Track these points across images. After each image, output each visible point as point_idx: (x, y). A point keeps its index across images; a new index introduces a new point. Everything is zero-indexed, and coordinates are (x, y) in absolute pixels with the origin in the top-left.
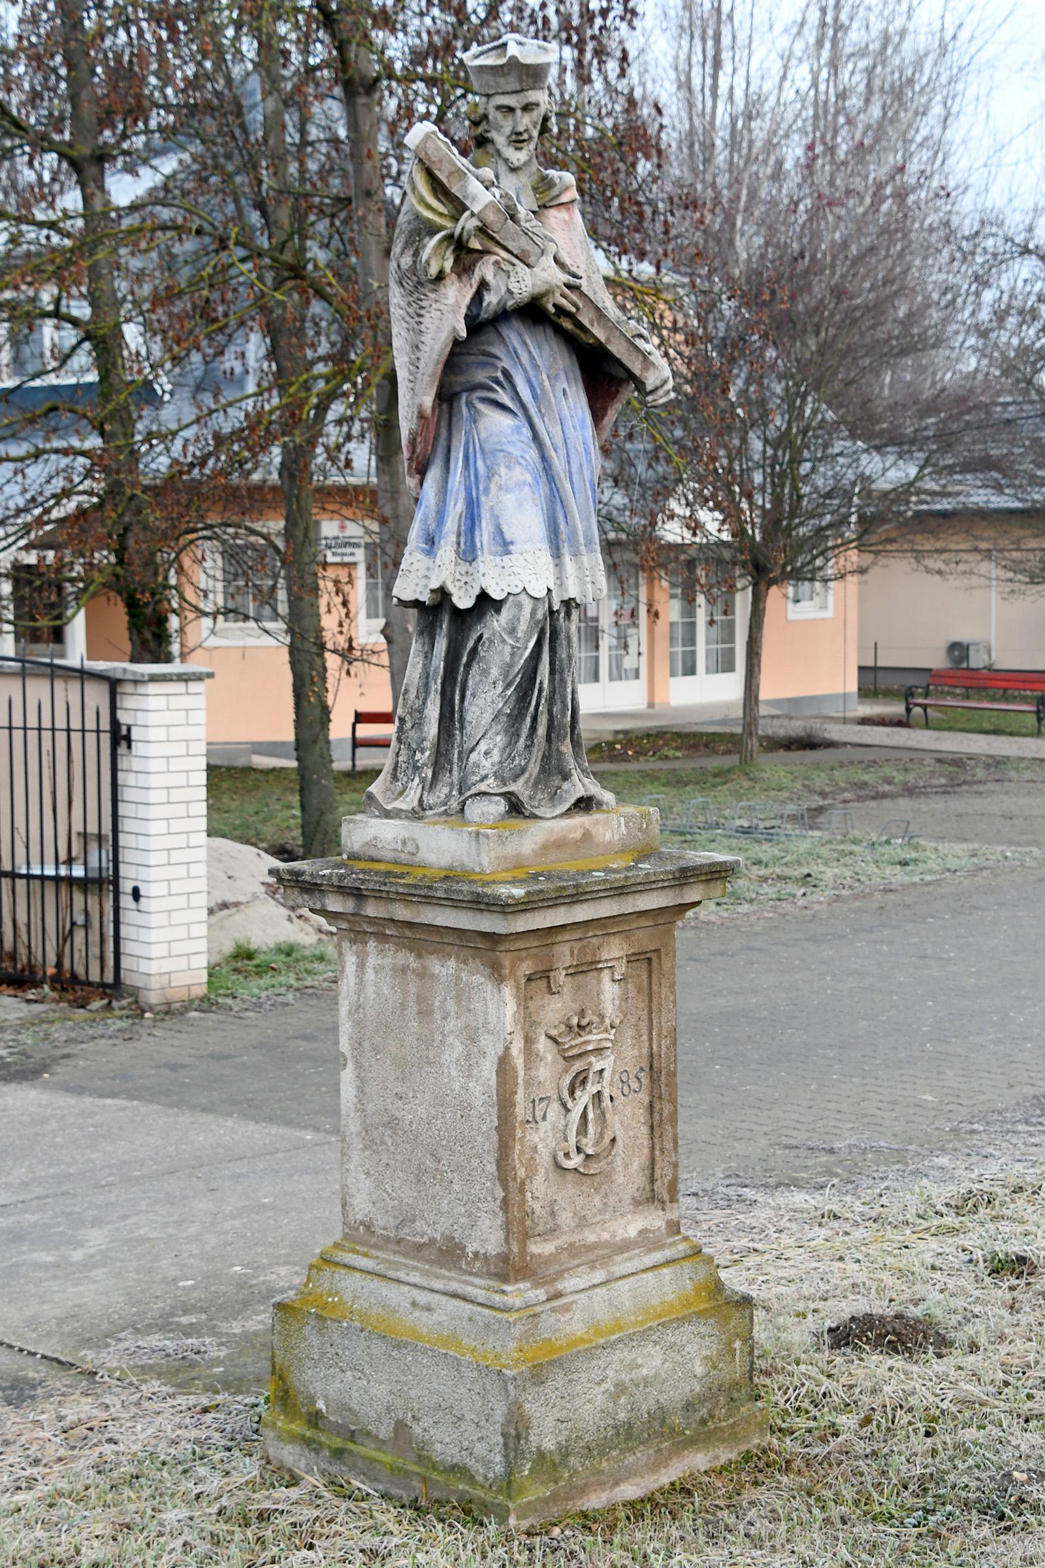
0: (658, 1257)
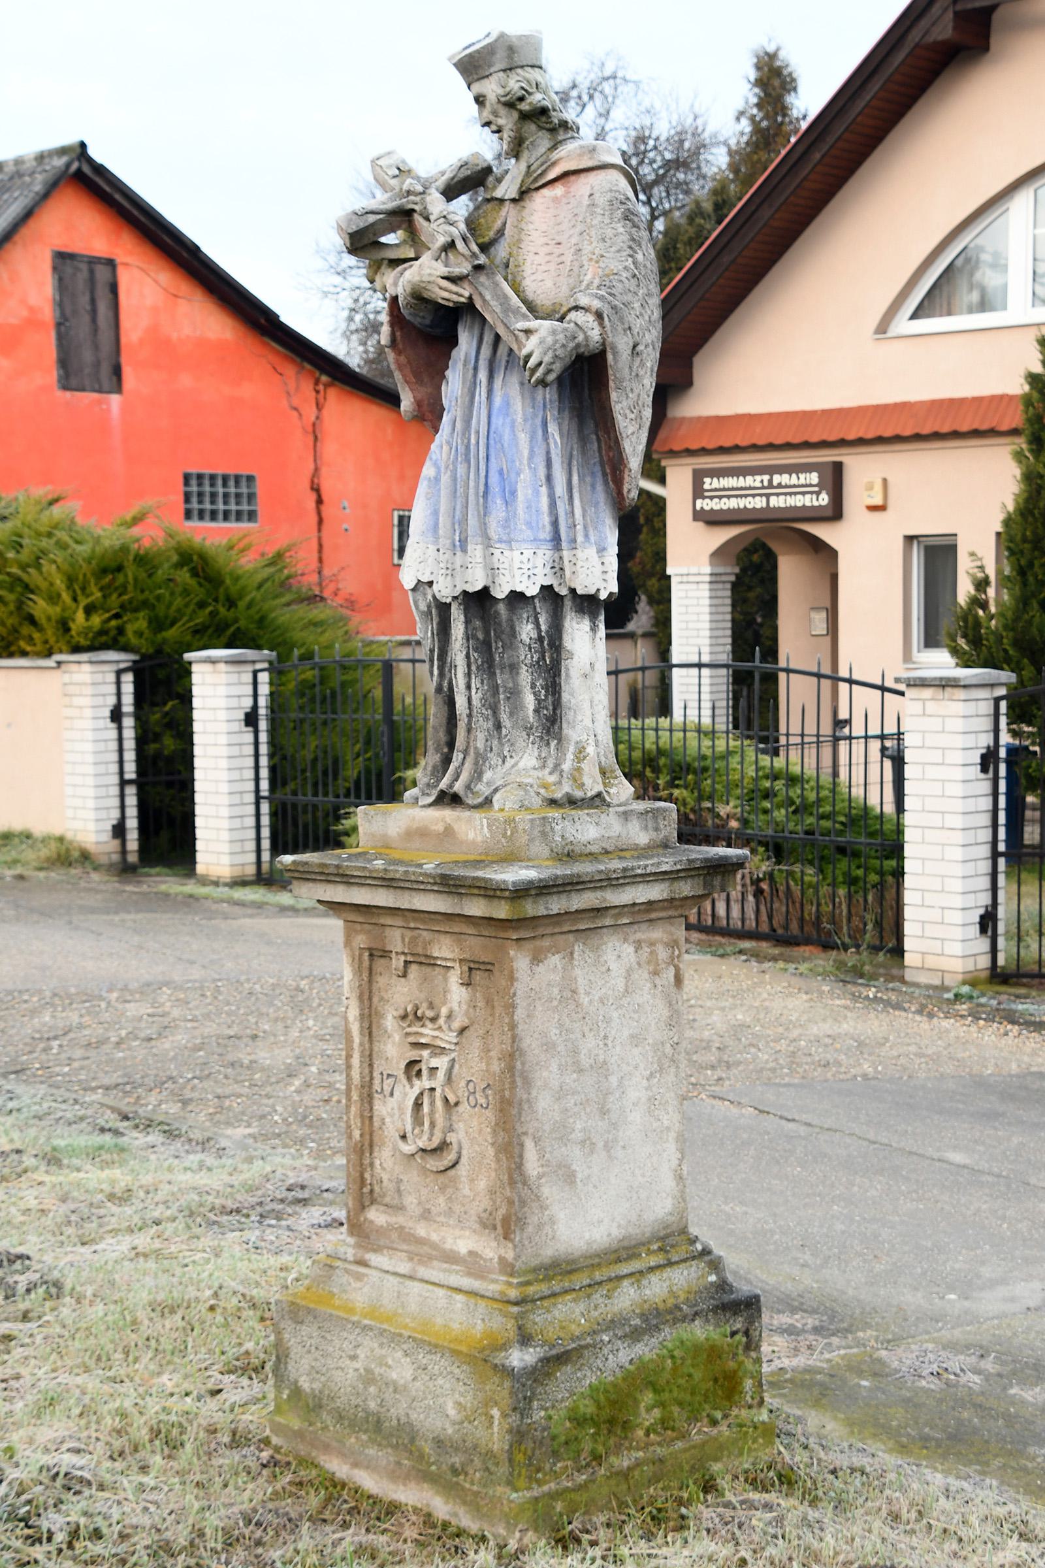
0: (467, 1282)
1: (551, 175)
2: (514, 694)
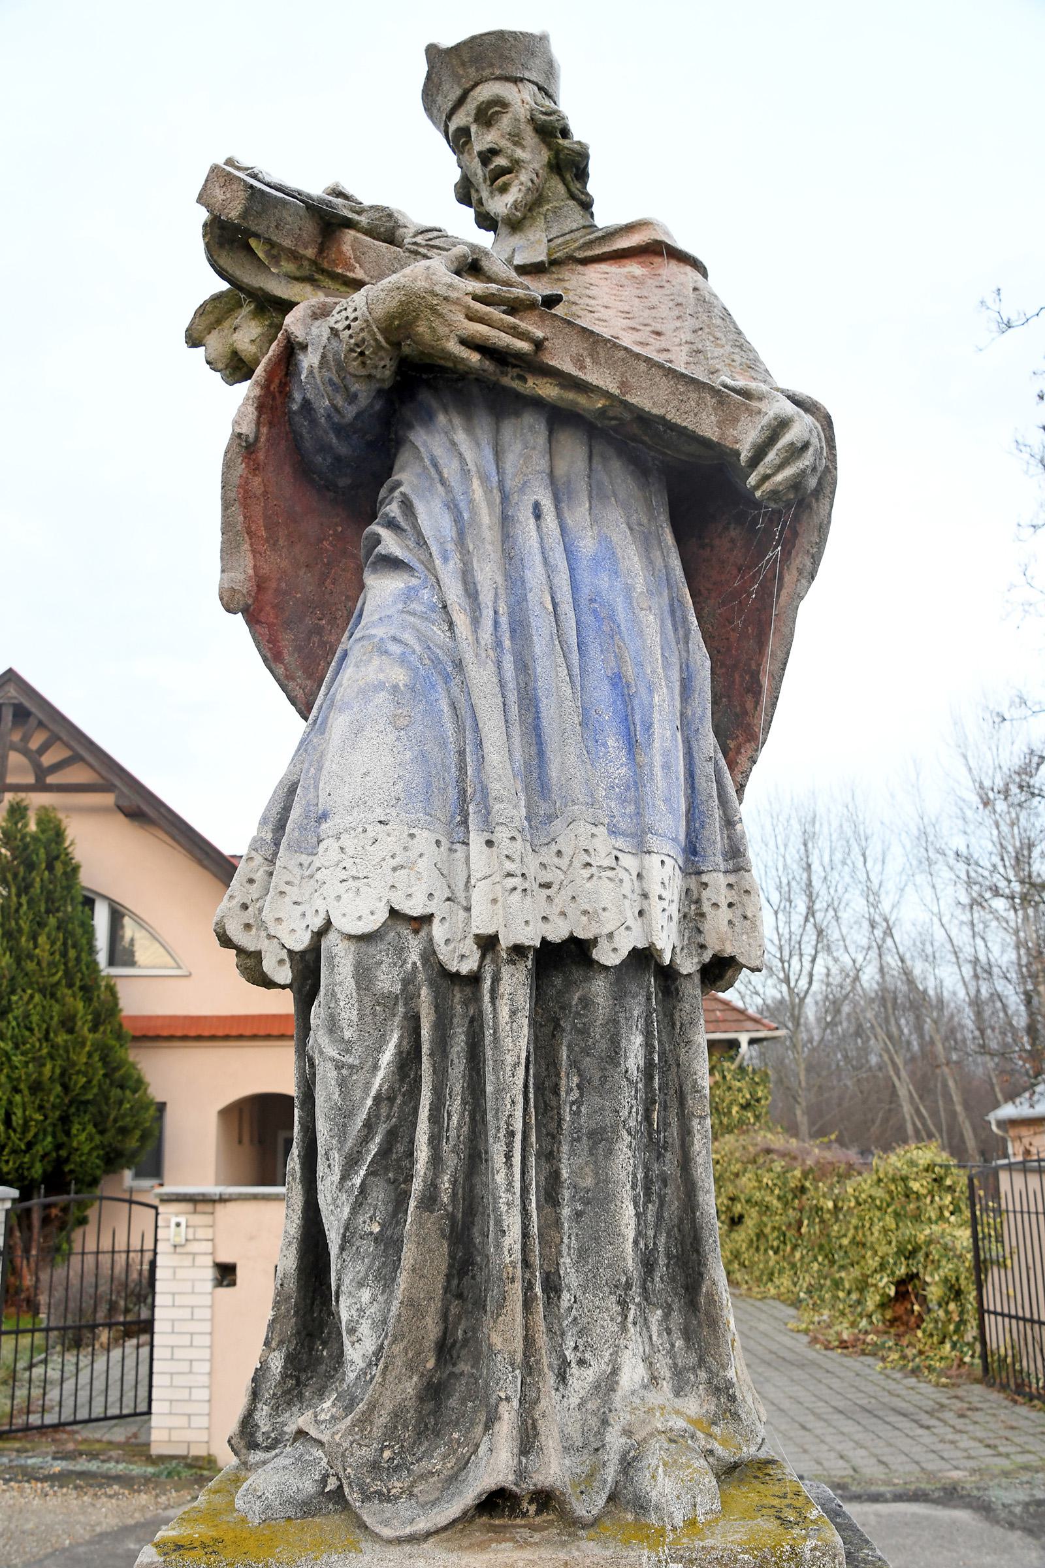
2: (598, 1200)
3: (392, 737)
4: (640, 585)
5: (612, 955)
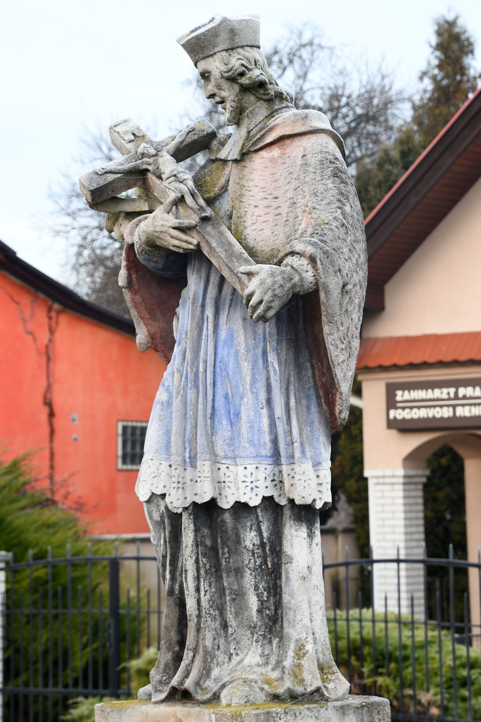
1: (269, 139)
2: (239, 595)
3: (158, 424)
4: (242, 349)
5: (227, 504)
